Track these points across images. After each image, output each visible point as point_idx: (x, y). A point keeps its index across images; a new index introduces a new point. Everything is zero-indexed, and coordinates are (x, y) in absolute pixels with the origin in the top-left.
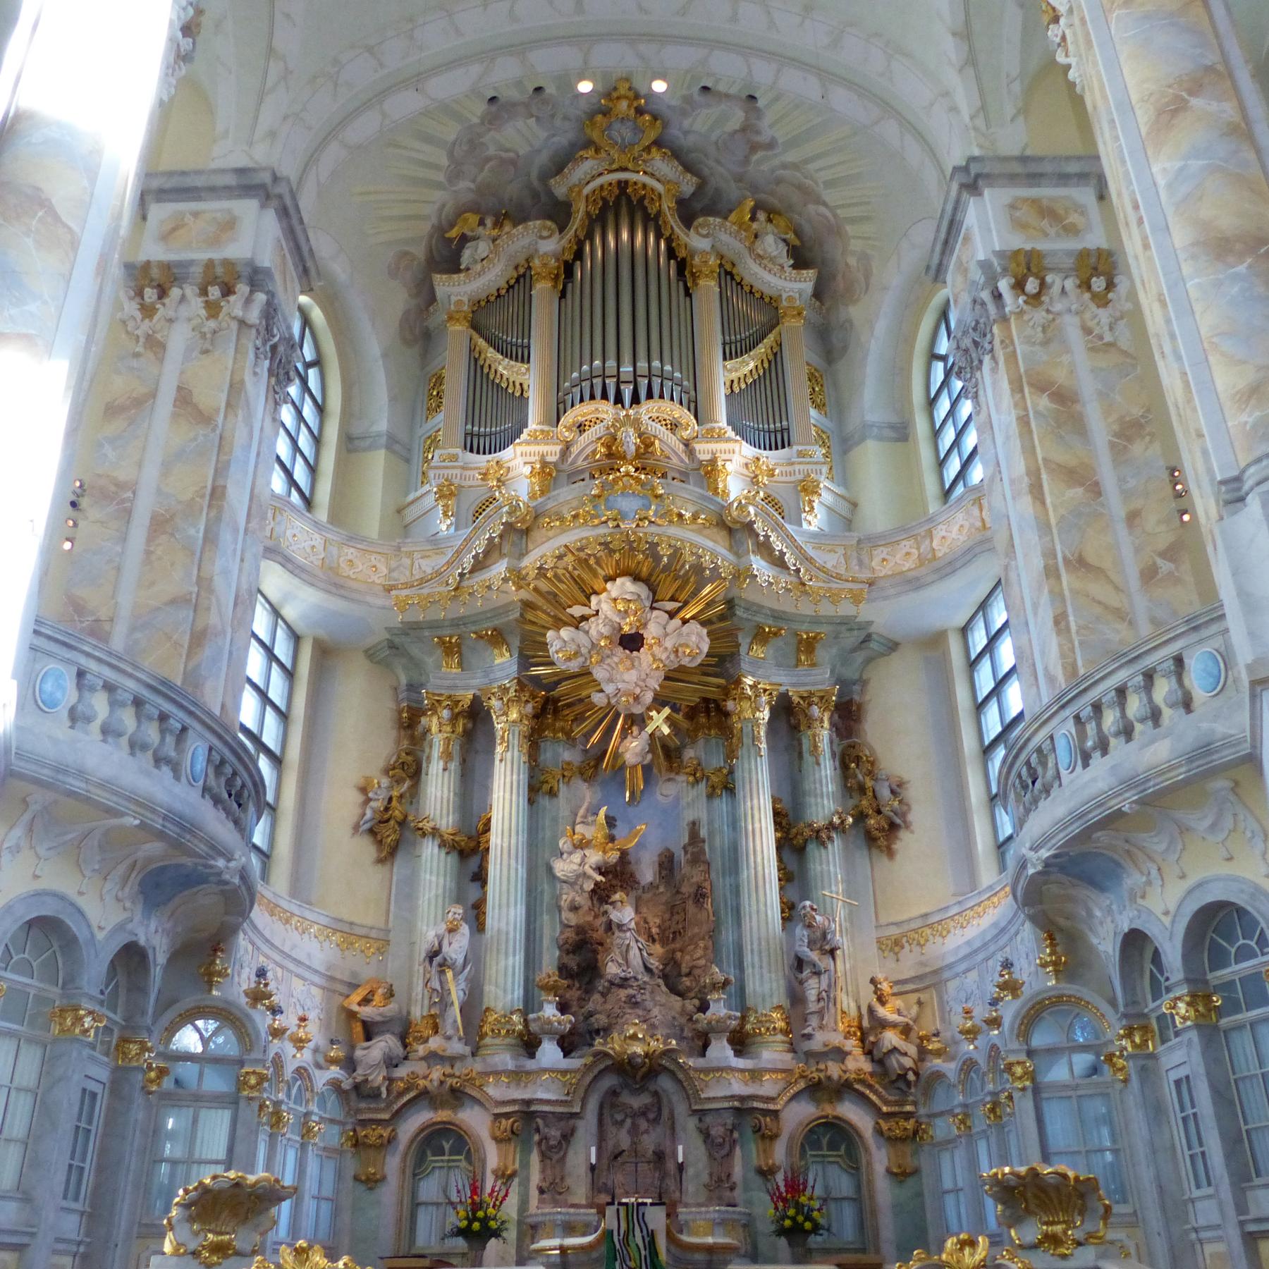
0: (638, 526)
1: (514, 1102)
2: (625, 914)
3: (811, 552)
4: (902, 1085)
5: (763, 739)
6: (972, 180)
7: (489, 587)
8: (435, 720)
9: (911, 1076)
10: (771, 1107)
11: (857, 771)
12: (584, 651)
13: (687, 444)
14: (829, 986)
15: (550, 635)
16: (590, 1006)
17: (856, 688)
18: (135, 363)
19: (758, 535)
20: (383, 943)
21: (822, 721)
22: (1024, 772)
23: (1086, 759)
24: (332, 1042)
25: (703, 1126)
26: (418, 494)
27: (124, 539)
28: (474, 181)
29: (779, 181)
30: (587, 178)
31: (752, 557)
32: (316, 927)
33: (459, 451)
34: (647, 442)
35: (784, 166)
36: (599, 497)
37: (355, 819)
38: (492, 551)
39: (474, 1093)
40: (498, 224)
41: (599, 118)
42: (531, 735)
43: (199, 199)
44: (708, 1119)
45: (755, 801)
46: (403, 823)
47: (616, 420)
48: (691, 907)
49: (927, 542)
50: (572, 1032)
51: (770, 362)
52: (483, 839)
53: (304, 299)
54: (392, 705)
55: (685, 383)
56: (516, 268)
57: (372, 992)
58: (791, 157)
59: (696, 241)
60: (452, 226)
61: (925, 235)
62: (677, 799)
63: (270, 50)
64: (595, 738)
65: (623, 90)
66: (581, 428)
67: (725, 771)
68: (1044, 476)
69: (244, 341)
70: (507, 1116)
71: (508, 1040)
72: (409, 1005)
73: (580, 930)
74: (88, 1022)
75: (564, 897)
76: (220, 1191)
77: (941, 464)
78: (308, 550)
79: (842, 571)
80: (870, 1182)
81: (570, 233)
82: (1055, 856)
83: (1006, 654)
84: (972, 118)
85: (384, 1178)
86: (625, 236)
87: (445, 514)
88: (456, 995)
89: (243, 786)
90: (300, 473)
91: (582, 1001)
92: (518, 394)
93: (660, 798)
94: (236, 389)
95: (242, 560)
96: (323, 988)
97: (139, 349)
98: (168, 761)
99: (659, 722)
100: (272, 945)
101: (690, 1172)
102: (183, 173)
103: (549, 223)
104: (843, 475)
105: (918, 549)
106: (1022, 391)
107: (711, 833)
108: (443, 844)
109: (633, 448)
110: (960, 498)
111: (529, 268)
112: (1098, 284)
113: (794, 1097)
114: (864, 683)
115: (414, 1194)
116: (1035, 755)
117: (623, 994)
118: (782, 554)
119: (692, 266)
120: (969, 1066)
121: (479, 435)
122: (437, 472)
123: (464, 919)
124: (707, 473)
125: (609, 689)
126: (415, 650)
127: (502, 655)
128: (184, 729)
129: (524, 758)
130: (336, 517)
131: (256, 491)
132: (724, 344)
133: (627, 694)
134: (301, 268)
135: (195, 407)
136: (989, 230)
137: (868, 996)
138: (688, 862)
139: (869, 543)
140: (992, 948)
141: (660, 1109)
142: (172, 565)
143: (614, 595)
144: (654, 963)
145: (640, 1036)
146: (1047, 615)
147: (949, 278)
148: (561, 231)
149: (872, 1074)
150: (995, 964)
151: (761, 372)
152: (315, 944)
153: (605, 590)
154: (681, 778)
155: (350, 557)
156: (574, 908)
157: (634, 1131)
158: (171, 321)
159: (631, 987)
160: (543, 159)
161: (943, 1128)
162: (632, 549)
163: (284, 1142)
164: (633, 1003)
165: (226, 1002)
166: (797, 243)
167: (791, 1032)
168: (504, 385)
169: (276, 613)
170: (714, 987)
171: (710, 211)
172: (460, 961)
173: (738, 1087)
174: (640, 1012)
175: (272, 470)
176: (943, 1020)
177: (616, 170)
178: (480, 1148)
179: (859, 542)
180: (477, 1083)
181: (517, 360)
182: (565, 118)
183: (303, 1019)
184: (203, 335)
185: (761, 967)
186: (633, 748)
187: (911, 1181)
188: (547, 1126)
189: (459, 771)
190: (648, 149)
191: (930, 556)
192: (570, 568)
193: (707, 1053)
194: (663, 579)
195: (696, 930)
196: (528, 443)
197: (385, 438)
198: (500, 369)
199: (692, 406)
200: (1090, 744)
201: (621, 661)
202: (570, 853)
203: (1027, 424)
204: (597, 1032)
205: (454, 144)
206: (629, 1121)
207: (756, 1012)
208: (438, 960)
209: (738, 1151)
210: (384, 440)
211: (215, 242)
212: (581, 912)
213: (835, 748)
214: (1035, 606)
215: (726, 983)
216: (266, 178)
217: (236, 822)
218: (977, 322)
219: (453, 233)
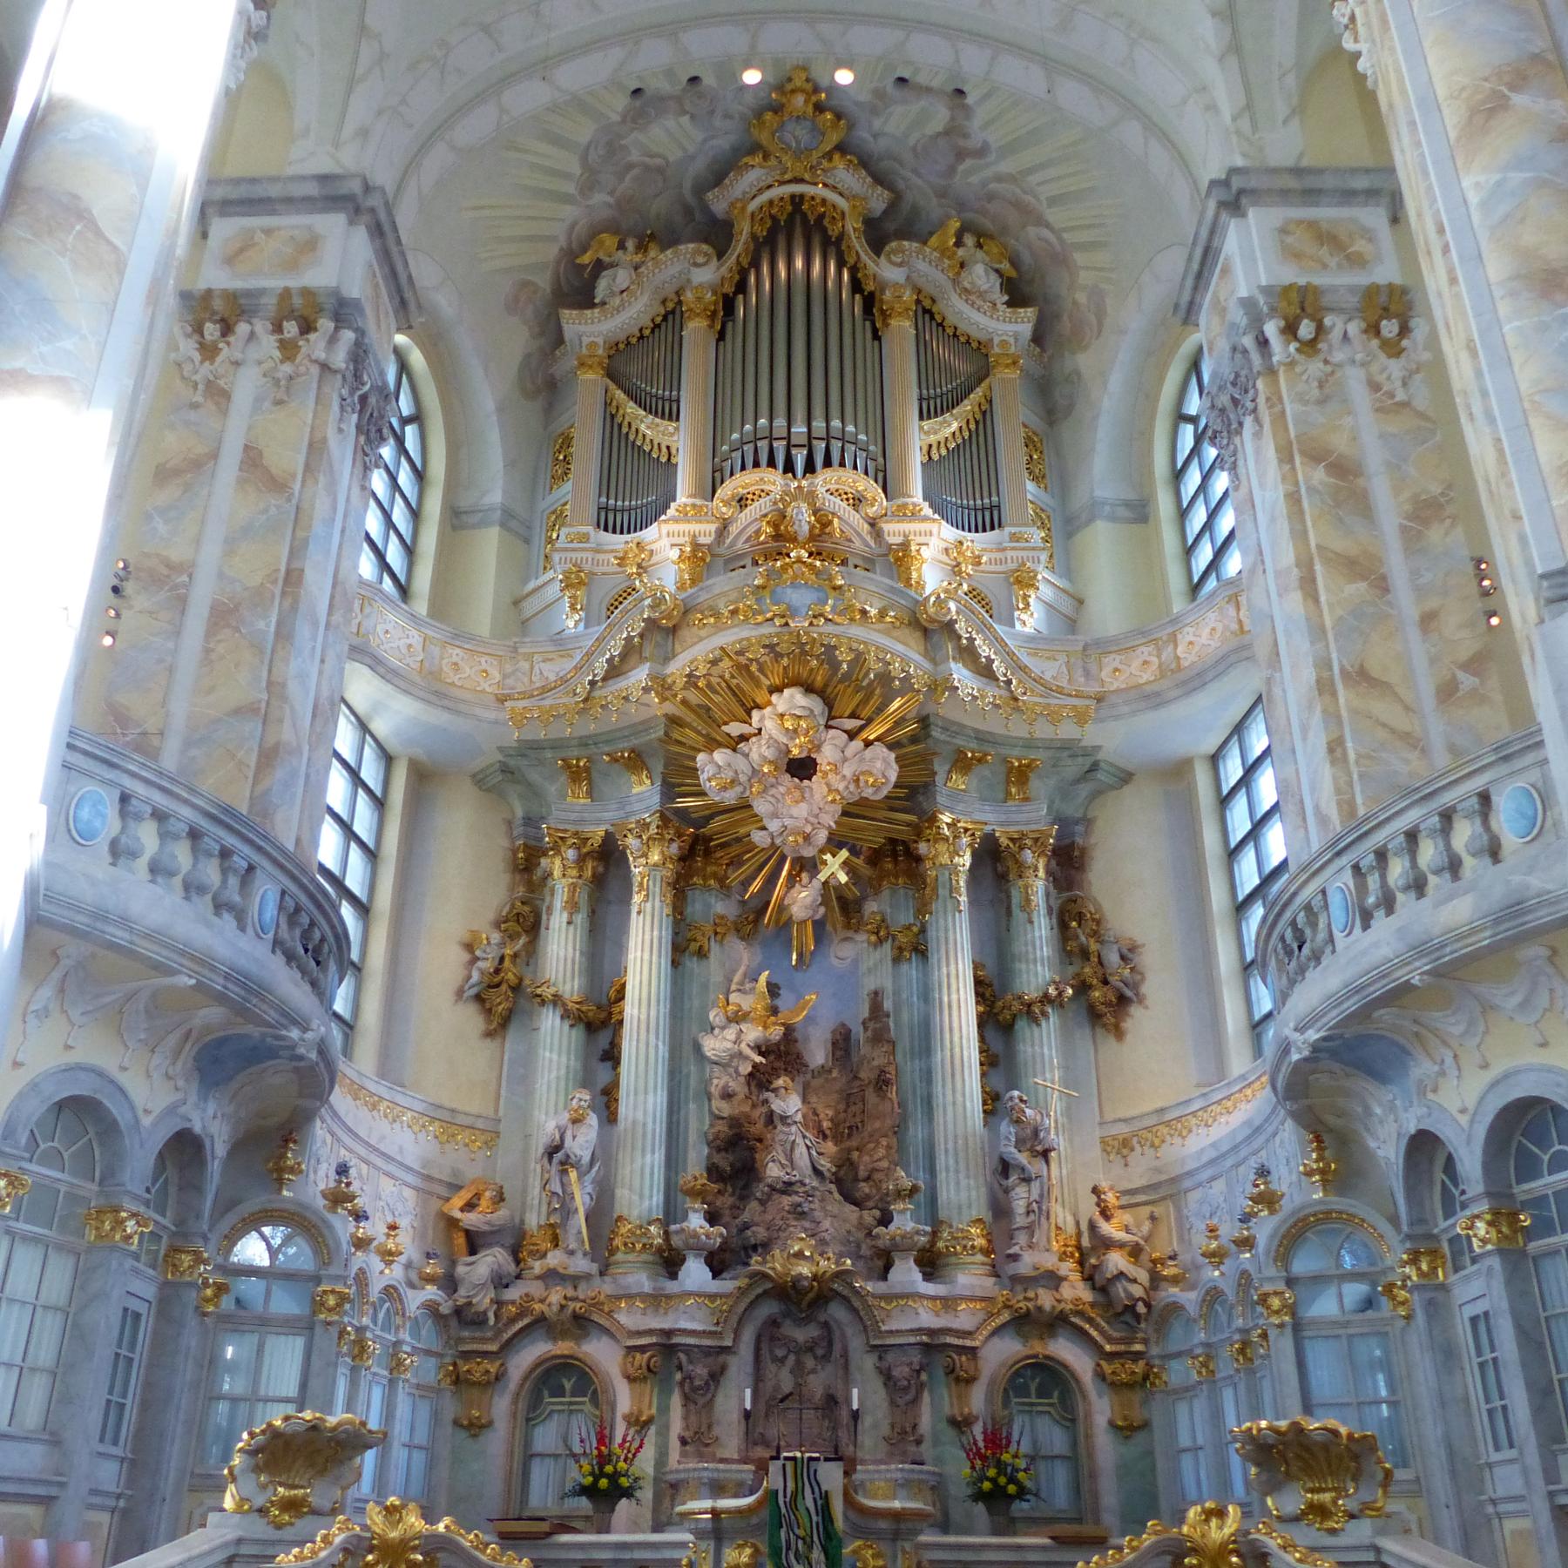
0: (811, 624)
1: (650, 1332)
3: (1026, 659)
4: (1128, 1318)
5: (963, 890)
6: (1233, 196)
7: (626, 699)
8: (558, 862)
9: (1141, 1309)
10: (968, 1343)
11: (1080, 931)
12: (743, 778)
13: (873, 523)
14: (1041, 1196)
16: (745, 1217)
17: (1080, 828)
18: (193, 416)
19: (960, 637)
20: (492, 1136)
21: (1036, 869)
22: (1289, 935)
23: (1366, 918)
24: (428, 1256)
25: (885, 1365)
26: (540, 581)
27: (178, 633)
28: (611, 193)
29: (991, 197)
30: (753, 190)
31: (952, 665)
32: (409, 1114)
33: (590, 529)
34: (823, 521)
35: (999, 178)
36: (764, 587)
38: (630, 653)
40: (642, 247)
41: (768, 116)
42: (677, 881)
43: (273, 213)
44: (890, 1357)
45: (953, 967)
46: (517, 988)
47: (786, 493)
48: (871, 1097)
49: (1171, 647)
50: (724, 1247)
51: (977, 422)
52: (615, 1009)
53: (400, 339)
54: (505, 843)
55: (872, 448)
56: (664, 302)
57: (478, 1196)
58: (1005, 167)
59: (888, 271)
60: (584, 250)
61: (1173, 264)
62: (856, 962)
63: (362, 30)
64: (755, 886)
65: (798, 82)
66: (742, 502)
67: (915, 929)
68: (1318, 567)
69: (326, 389)
70: (642, 1349)
71: (644, 1257)
72: (523, 1213)
73: (734, 1122)
74: (130, 1226)
75: (715, 1081)
76: (295, 1435)
77: (1189, 551)
78: (404, 651)
79: (1064, 683)
80: (1088, 1437)
81: (731, 260)
82: (1324, 1039)
83: (1266, 788)
84: (1234, 119)
85: (490, 1424)
86: (799, 263)
87: (573, 607)
88: (581, 1200)
89: (323, 939)
90: (394, 555)
91: (736, 1209)
92: (664, 459)
93: (835, 962)
94: (316, 449)
95: (322, 661)
96: (414, 1188)
97: (198, 398)
98: (230, 907)
99: (835, 868)
100: (356, 1135)
101: (866, 1422)
102: (253, 181)
103: (705, 247)
104: (1066, 564)
105: (1159, 656)
106: (1291, 460)
107: (897, 1006)
109: (806, 528)
110: (1213, 593)
111: (680, 303)
112: (1389, 328)
113: (996, 1332)
114: (1088, 822)
115: (527, 1442)
116: (1302, 914)
117: (786, 1201)
118: (990, 661)
119: (882, 301)
120: (1213, 1296)
121: (615, 510)
122: (563, 555)
123: (592, 1107)
124: (898, 559)
125: (774, 826)
126: (534, 776)
127: (641, 783)
128: (251, 868)
129: (668, 910)
130: (441, 607)
131: (341, 576)
132: (921, 399)
133: (795, 832)
134: (397, 300)
135: (267, 471)
136: (1255, 260)
137: (1089, 1209)
138: (867, 1040)
139: (1099, 648)
140: (1243, 1154)
141: (830, 1343)
142: (236, 666)
143: (780, 709)
144: (825, 1165)
145: (807, 1253)
146: (1319, 739)
147: (1203, 320)
148: (720, 255)
149: (1092, 1305)
150: (1248, 1173)
151: (966, 435)
152: (408, 1135)
153: (769, 703)
154: (861, 937)
155: (455, 659)
156: (727, 1096)
157: (798, 1370)
158: (237, 364)
159: (797, 1193)
160: (699, 166)
161: (1179, 1373)
162: (804, 653)
163: (369, 1377)
164: (799, 1213)
165: (301, 1205)
166: (1013, 274)
167: (993, 1252)
168: (647, 448)
169: (363, 727)
170: (899, 1194)
171: (905, 234)
172: (586, 1159)
173: (927, 1318)
174: (807, 1224)
175: (360, 549)
176: (1181, 1239)
177: (790, 182)
179: (1085, 648)
180: (606, 1309)
181: (663, 417)
182: (727, 116)
183: (393, 1227)
184: (277, 382)
185: (957, 1171)
186: (802, 900)
187: (1140, 1437)
188: (690, 1362)
189: (587, 925)
190: (829, 156)
191: (1173, 666)
192: (727, 676)
193: (890, 1276)
194: (841, 690)
195: (877, 1125)
196: (675, 520)
197: (499, 512)
198: (643, 427)
199: (880, 475)
200: (1371, 900)
201: (789, 792)
202: (723, 1028)
203: (1299, 501)
204: (755, 1248)
206: (792, 1358)
207: (951, 1226)
208: (559, 1156)
209: (926, 1397)
211: (292, 265)
212: (735, 1100)
213: (1052, 902)
214: (1305, 730)
215: (914, 1190)
216: (355, 187)
217: (314, 984)
218: (1237, 375)
219: (586, 259)
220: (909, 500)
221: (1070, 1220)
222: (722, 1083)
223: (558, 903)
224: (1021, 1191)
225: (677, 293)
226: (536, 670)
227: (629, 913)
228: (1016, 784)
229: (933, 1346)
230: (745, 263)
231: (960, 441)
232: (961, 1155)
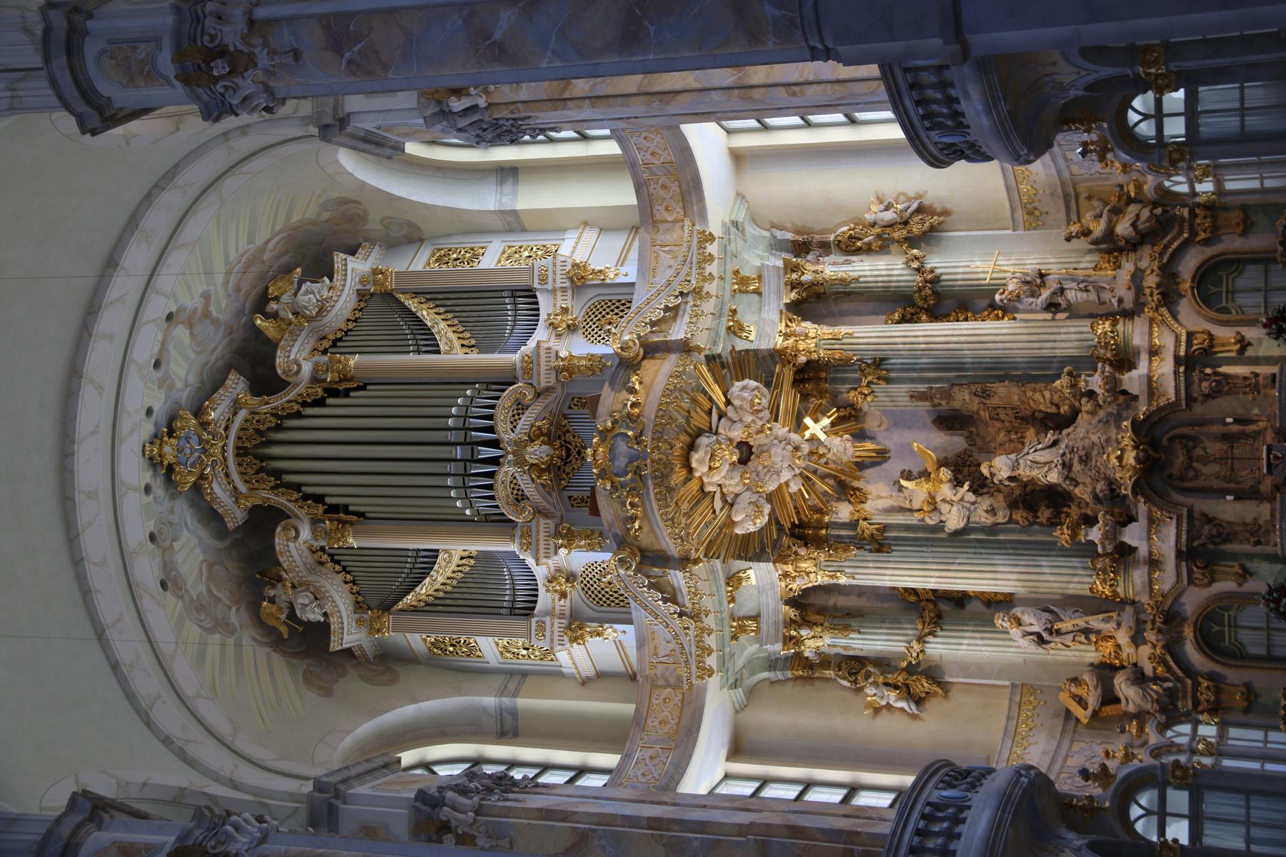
1: (1178, 567)
2: (1000, 467)
5: (836, 329)
8: (808, 643)
10: (1184, 338)
11: (866, 240)
13: (538, 395)
14: (1074, 280)
15: (739, 531)
17: (780, 235)
24: (1123, 731)
28: (230, 608)
29: (238, 290)
35: (226, 283)
37: (906, 718)
39: (1169, 603)
48: (995, 401)
51: (437, 306)
56: (322, 564)
72: (1082, 664)
73: (1012, 505)
78: (656, 762)
92: (472, 562)
96: (1072, 741)
99: (816, 427)
103: (279, 529)
108: (932, 633)
109: (545, 447)
114: (774, 226)
115: (1259, 658)
117: (1077, 467)
118: (667, 309)
121: (514, 601)
122: (556, 642)
125: (786, 476)
132: (419, 352)
137: (1082, 244)
144: (1051, 437)
148: (289, 517)
151: (450, 316)
153: (700, 478)
155: (656, 723)
157: (1205, 461)
164: (1086, 460)
170: (1073, 386)
172: (1047, 615)
174: (1095, 452)
177: (225, 459)
188: (1199, 538)
195: (1016, 398)
198: (441, 579)
205: (201, 627)
206: (1195, 464)
208: (1045, 635)
209: (1224, 369)
210: (506, 701)
213: (842, 259)
215: (1070, 374)
220: (518, 365)
221: (1088, 258)
222: (984, 514)
224: (1071, 295)
225: (314, 552)
227: (851, 586)
228: (748, 285)
230: (296, 495)
231: (456, 321)
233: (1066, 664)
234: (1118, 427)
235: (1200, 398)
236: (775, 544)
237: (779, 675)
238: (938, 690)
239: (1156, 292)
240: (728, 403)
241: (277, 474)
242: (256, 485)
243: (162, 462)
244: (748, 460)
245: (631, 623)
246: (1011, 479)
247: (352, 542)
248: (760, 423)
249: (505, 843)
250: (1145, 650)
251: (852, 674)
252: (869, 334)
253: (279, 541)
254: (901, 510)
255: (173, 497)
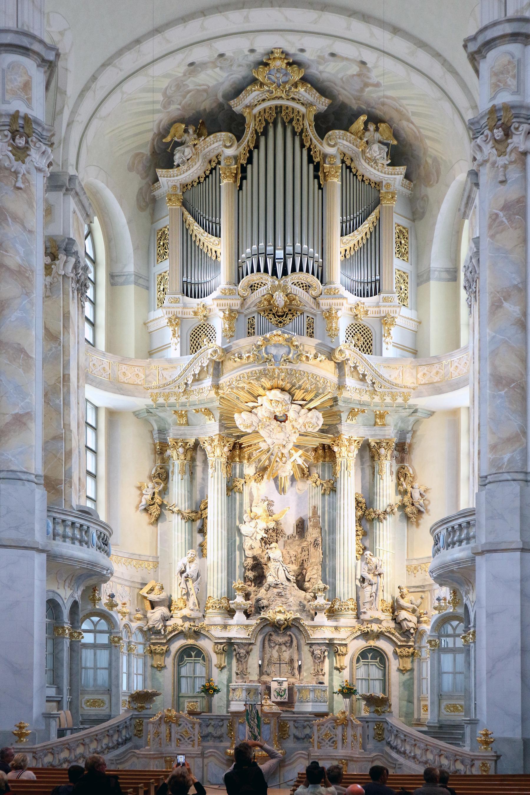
2: (276, 552)
8: (175, 452)
10: (344, 642)
20: (156, 565)
33: (180, 296)
37: (137, 503)
46: (162, 506)
47: (273, 287)
66: (253, 288)
75: (247, 544)
79: (399, 381)
85: (165, 666)
108: (183, 518)
109: (283, 303)
117: (276, 591)
125: (269, 441)
155: (124, 370)
177: (274, 99)
178: (209, 656)
222: (249, 545)
223: (176, 471)
226: (160, 373)
229: (330, 644)
230: (252, 146)
232: (346, 575)
233: (171, 583)
234: (297, 611)
235: (312, 650)
236: (230, 435)
237: (156, 436)
238: (153, 520)
239: (369, 630)
240: (310, 410)
241: (265, 133)
242: (258, 120)
243: (270, 59)
244: (277, 420)
245: (181, 355)
246: (269, 558)
247: (224, 182)
248: (298, 427)
249: (48, 293)
250: (180, 622)
251: (159, 475)
252: (350, 485)
253: (223, 135)
254: (251, 501)
255: (248, 66)
